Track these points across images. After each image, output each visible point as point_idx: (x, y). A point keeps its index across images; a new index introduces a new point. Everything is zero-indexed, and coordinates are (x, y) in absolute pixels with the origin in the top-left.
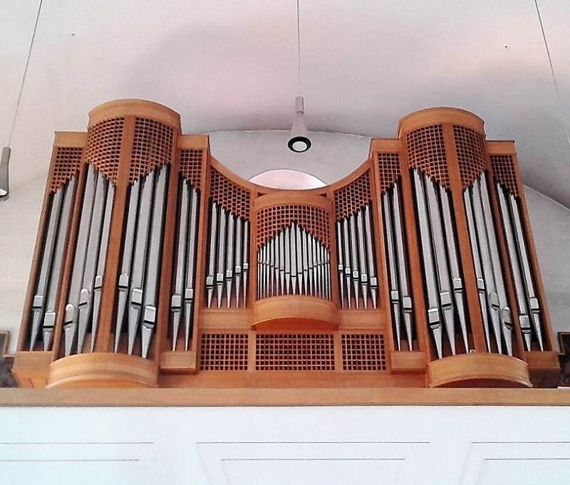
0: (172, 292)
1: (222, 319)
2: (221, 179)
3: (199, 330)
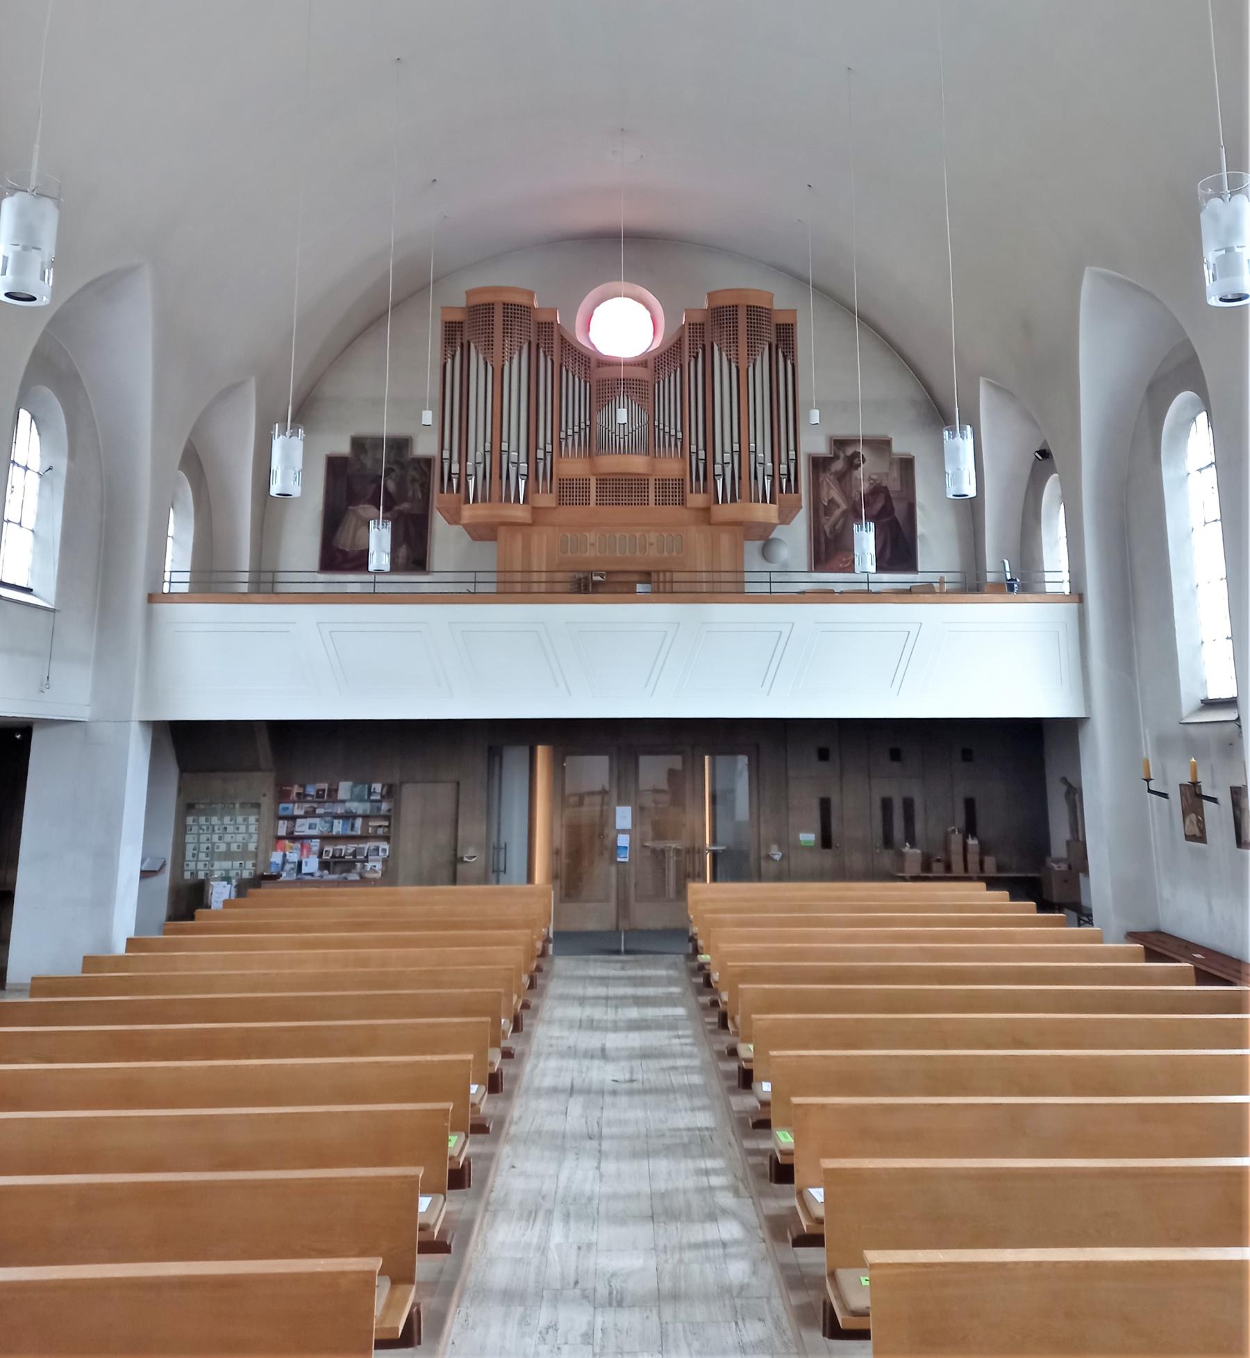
0: (537, 448)
1: (573, 466)
2: (569, 346)
3: (557, 475)
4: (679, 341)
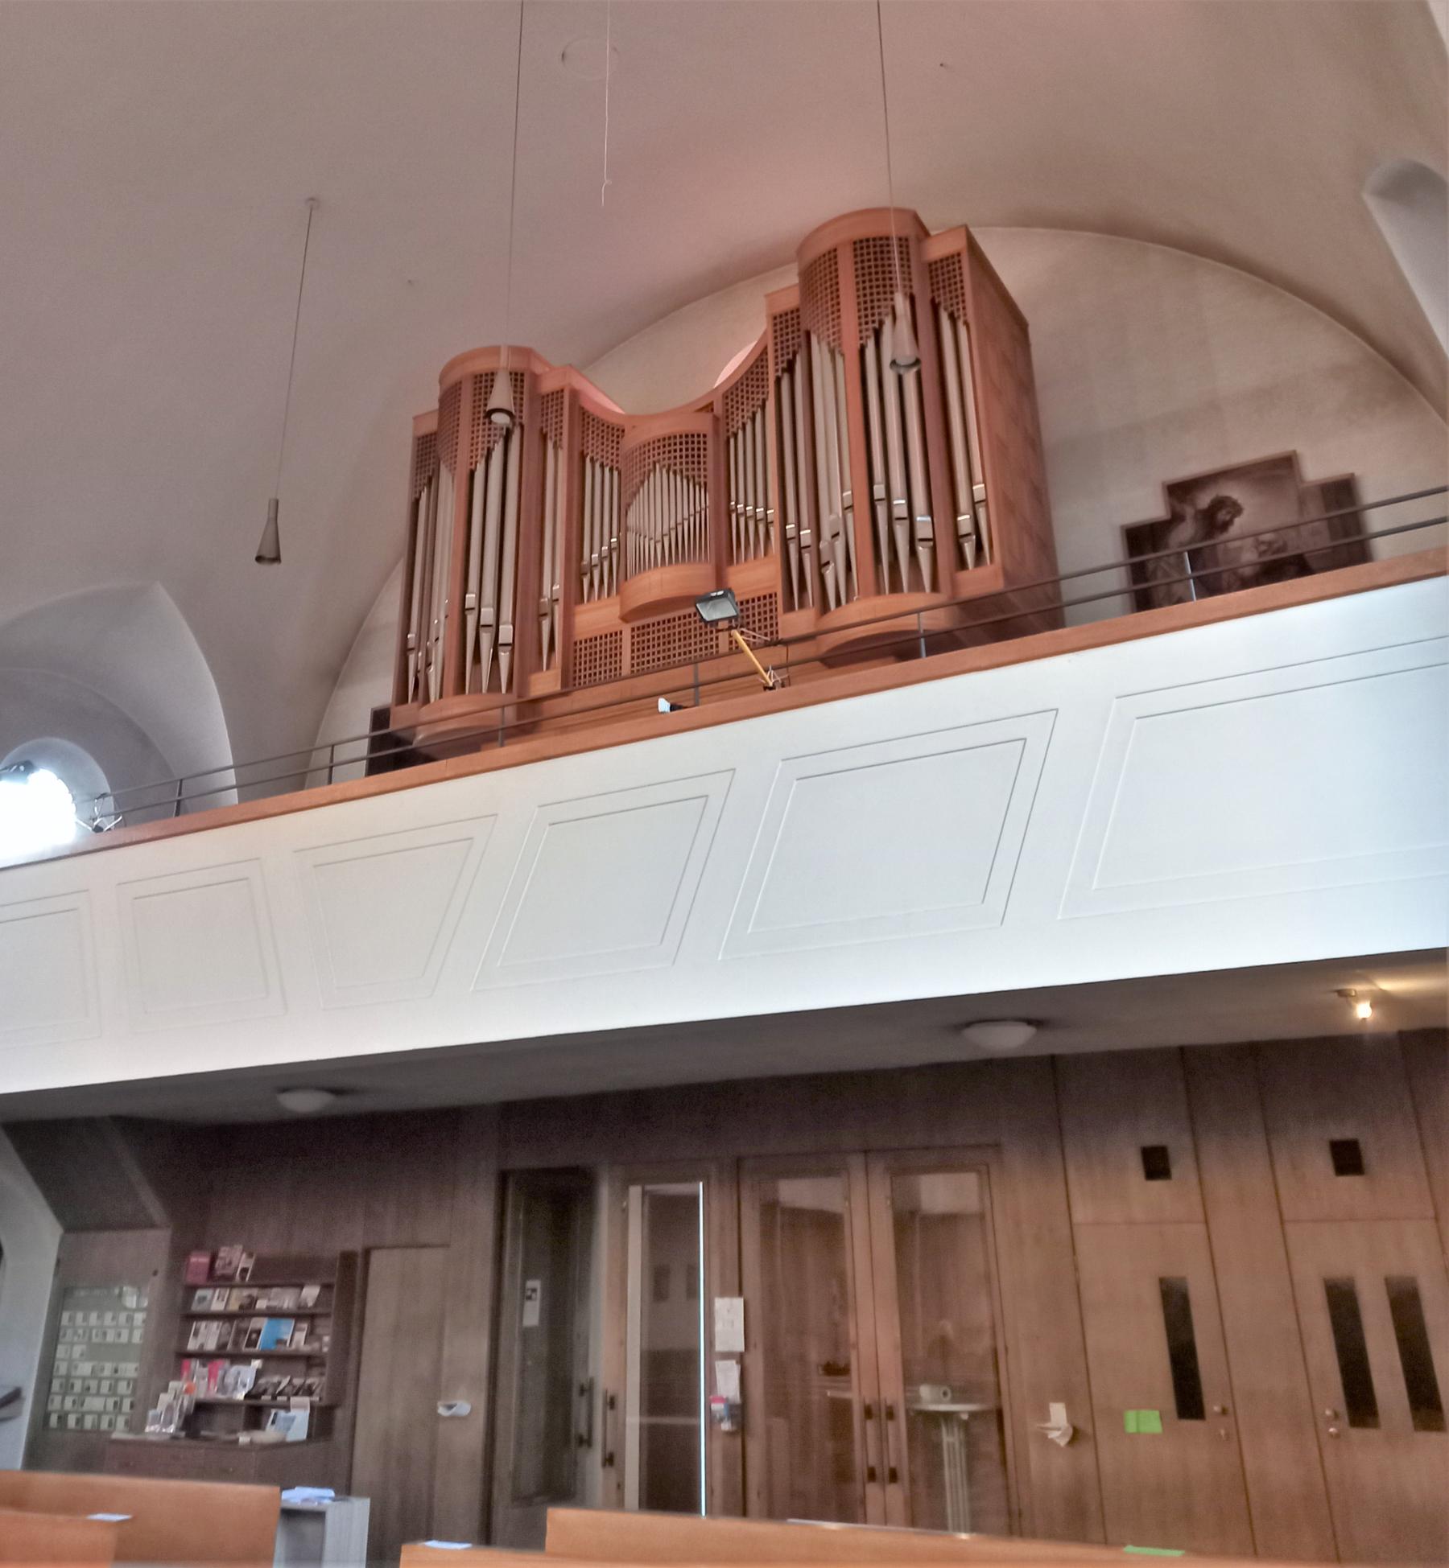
4: (765, 351)
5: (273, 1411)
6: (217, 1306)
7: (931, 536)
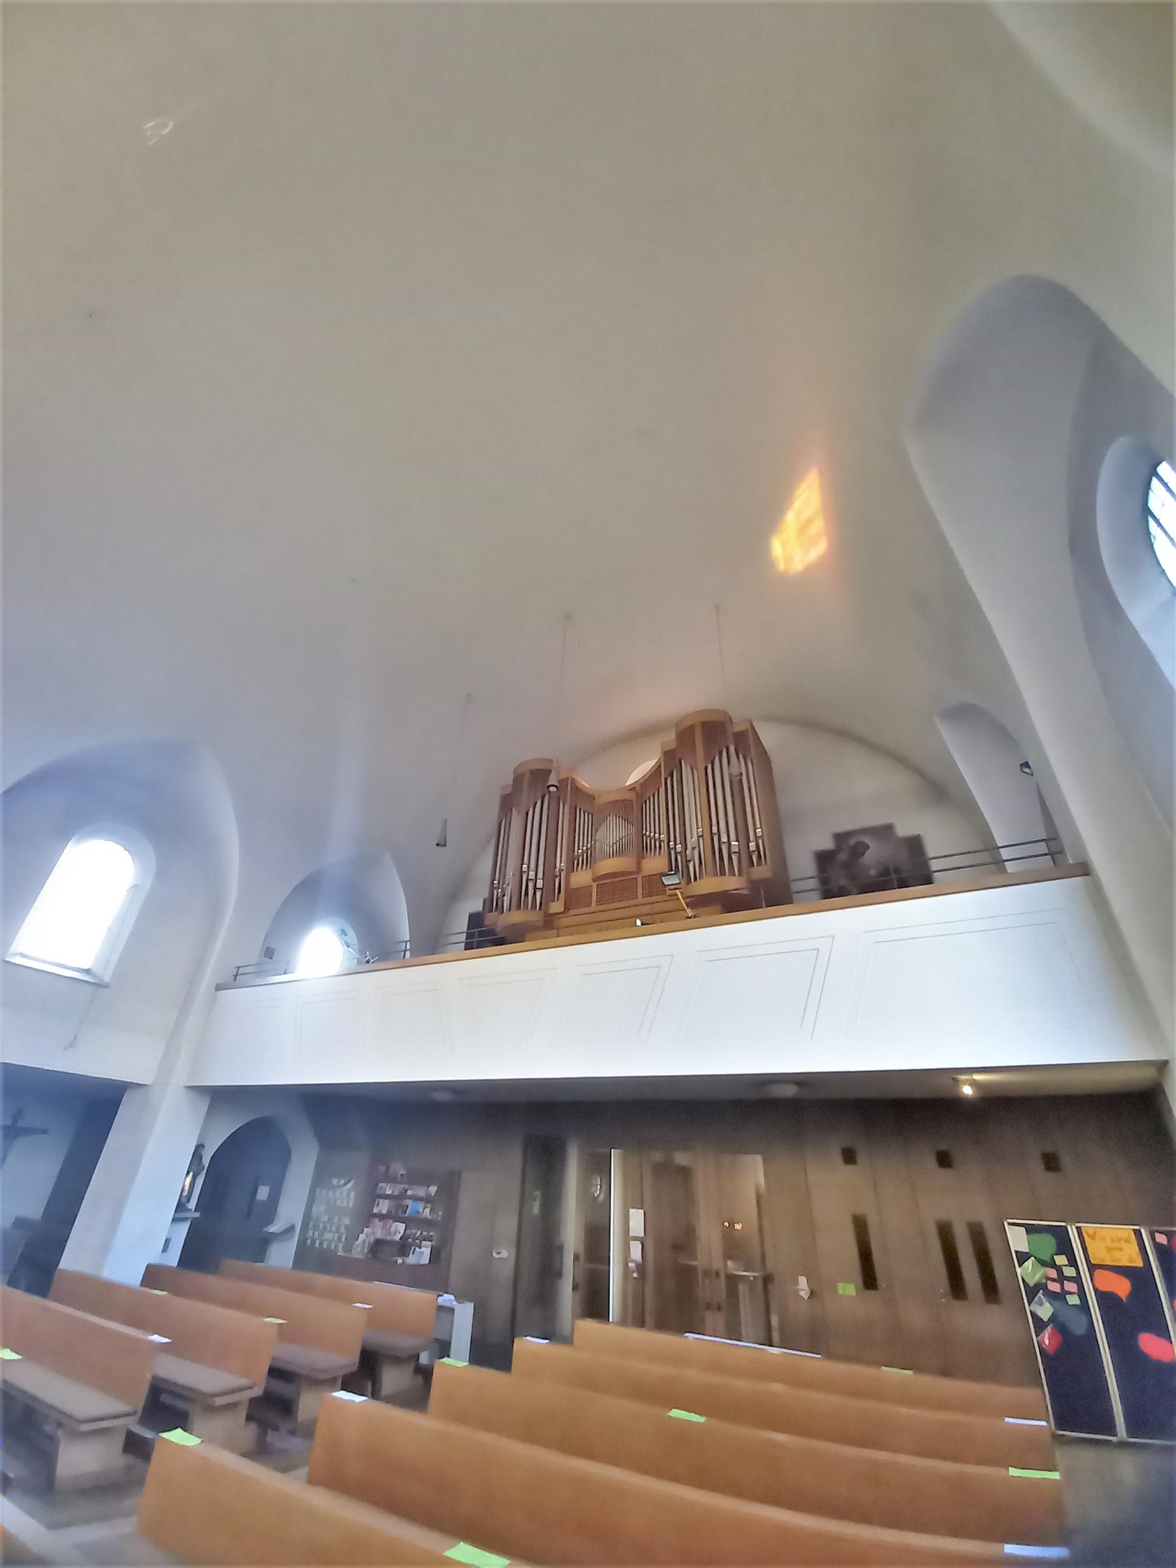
1: (582, 878)
5: (413, 1248)
6: (388, 1192)
7: (738, 851)
